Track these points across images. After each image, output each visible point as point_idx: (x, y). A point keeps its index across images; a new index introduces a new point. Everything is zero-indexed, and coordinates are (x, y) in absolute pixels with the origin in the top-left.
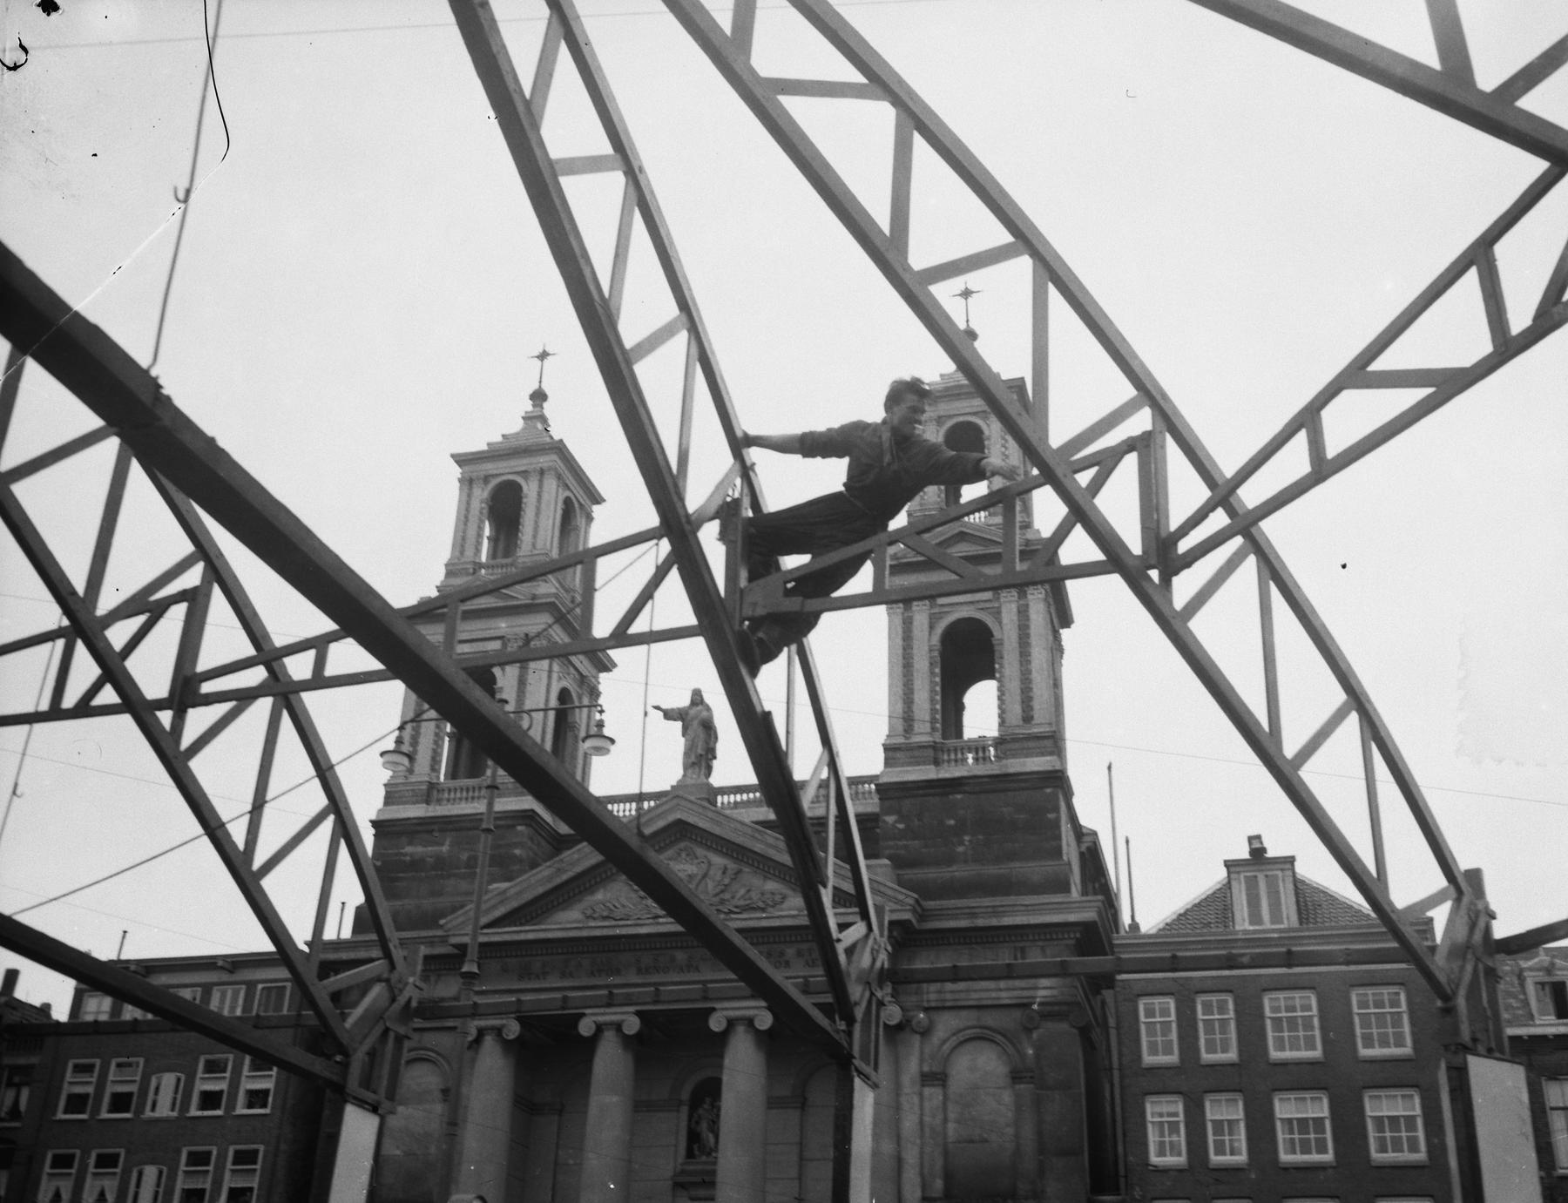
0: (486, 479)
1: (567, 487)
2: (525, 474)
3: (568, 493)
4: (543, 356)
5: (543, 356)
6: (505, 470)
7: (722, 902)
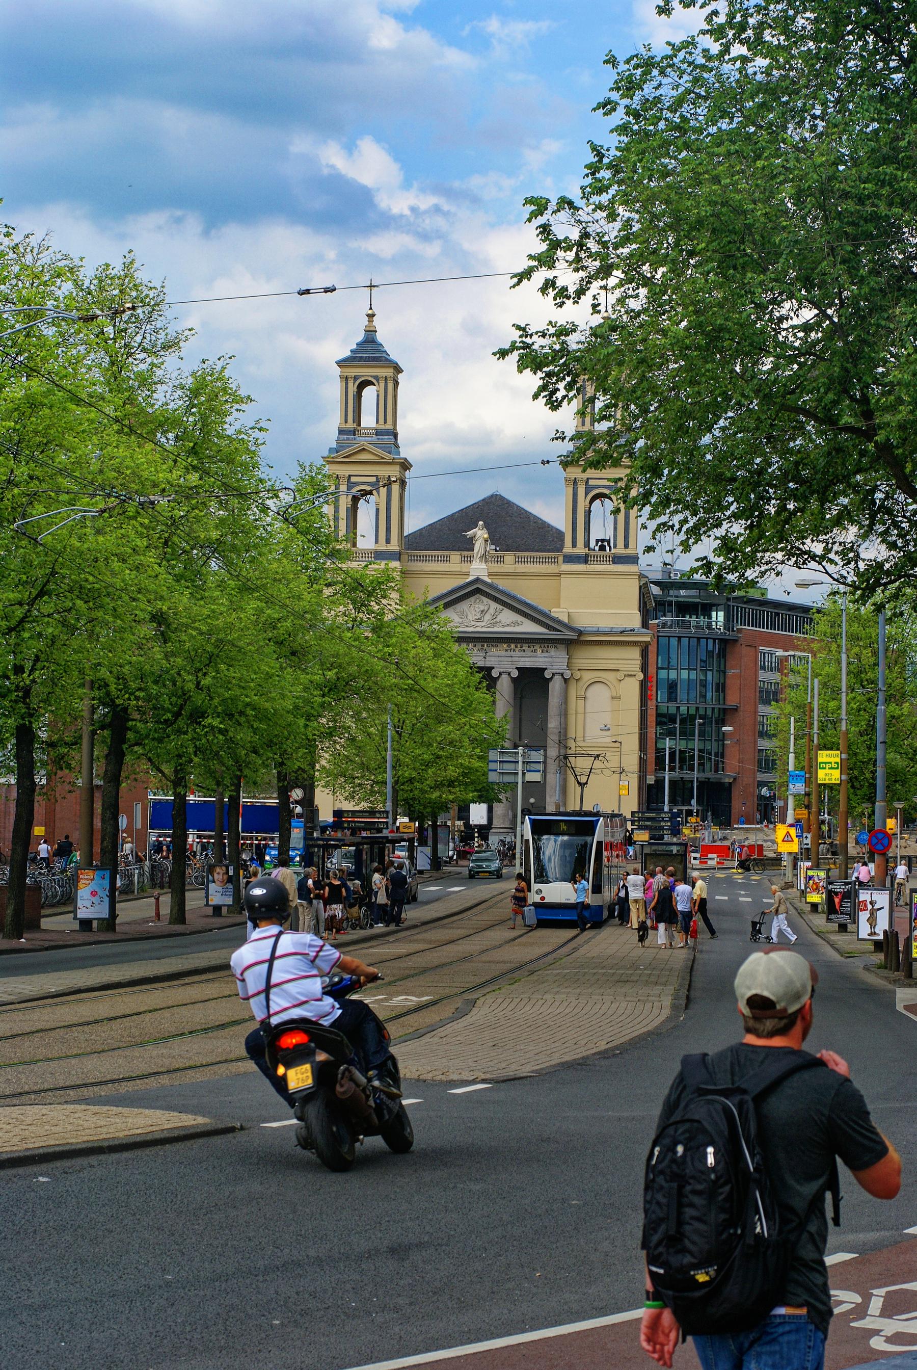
0: (355, 378)
2: (376, 378)
6: (366, 372)
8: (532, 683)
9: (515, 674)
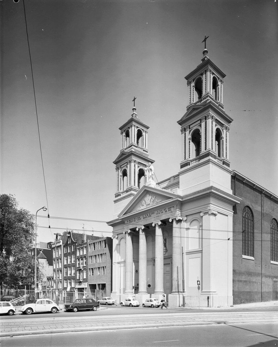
1: (137, 127)
3: (138, 129)
8: (167, 226)
9: (160, 223)
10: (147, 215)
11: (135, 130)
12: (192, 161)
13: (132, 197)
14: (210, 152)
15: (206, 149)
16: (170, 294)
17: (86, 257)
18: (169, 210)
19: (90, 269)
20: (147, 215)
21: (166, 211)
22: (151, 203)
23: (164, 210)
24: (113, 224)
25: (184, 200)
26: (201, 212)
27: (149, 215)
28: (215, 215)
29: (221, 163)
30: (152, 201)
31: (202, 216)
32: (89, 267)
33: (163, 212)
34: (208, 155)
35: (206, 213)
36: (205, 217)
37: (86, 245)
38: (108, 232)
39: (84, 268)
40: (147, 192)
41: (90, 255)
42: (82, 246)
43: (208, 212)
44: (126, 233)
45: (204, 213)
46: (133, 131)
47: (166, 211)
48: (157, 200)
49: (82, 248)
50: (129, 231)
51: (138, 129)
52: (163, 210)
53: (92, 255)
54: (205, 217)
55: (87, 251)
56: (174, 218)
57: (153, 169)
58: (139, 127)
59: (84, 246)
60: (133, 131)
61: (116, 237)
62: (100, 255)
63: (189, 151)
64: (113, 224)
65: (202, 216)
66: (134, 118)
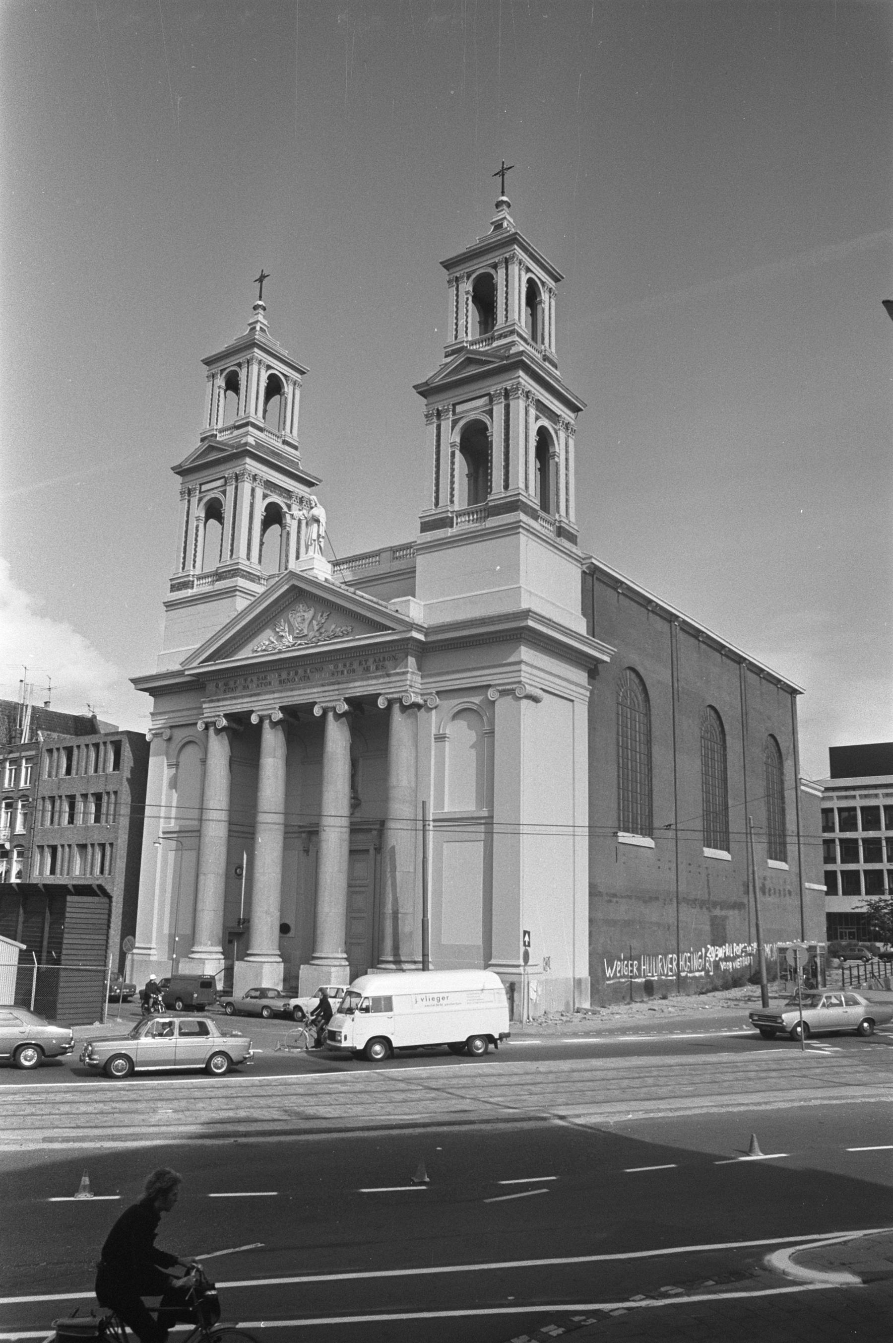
0: (222, 371)
2: (239, 365)
3: (270, 372)
4: (261, 279)
5: (261, 279)
7: (321, 633)
10: (296, 674)
11: (259, 375)
12: (460, 514)
13: (241, 603)
14: (521, 497)
15: (506, 487)
16: (242, 960)
17: (31, 800)
18: (377, 669)
19: (41, 847)
20: (296, 674)
21: (367, 670)
22: (311, 634)
23: (360, 664)
24: (158, 688)
25: (430, 639)
26: (489, 686)
27: (301, 671)
28: (536, 700)
29: (549, 532)
30: (316, 628)
31: (494, 702)
32: (38, 841)
33: (354, 671)
34: (514, 505)
35: (503, 693)
36: (503, 705)
37: (33, 753)
38: (136, 715)
39: (15, 843)
40: (299, 593)
41: (47, 794)
42: (11, 756)
43: (513, 690)
44: (207, 728)
45: (500, 692)
46: (255, 380)
47: (367, 670)
48: (333, 627)
49: (16, 762)
50: (224, 722)
51: (270, 372)
52: (355, 666)
53: (55, 793)
54: (503, 705)
55: (35, 778)
56: (395, 696)
57: (323, 520)
58: (273, 368)
59: (23, 754)
60: (255, 380)
61: (167, 733)
62: (90, 796)
63: (452, 483)
64: (158, 688)
65: (494, 702)
66: (258, 336)
